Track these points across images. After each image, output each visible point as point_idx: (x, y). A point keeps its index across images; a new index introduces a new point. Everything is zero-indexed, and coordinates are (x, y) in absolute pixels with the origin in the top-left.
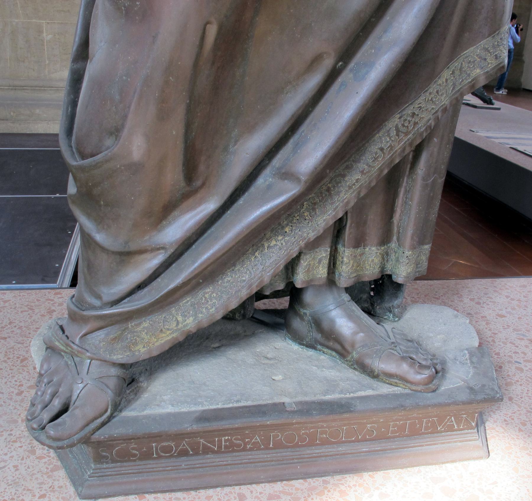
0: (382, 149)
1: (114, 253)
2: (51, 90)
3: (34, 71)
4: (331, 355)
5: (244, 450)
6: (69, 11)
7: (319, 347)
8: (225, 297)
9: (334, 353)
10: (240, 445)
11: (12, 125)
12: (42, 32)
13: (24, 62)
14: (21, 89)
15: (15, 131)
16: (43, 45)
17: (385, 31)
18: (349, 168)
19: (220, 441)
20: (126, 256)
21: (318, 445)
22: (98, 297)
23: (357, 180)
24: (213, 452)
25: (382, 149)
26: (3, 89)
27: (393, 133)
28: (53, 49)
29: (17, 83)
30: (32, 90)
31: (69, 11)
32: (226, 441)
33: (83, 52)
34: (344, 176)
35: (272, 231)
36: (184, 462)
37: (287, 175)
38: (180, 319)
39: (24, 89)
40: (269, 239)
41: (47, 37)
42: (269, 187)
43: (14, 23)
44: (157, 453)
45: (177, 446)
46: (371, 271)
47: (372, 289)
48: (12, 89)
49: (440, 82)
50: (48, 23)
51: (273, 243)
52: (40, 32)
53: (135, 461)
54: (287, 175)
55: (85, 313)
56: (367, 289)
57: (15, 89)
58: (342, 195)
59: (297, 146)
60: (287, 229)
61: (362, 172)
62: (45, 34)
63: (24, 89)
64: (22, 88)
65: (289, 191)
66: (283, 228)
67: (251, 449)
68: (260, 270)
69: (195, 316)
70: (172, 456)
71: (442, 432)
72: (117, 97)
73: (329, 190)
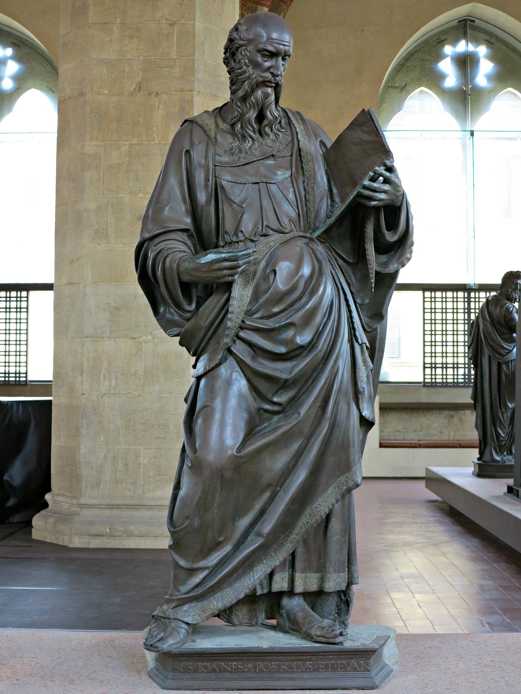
0: (304, 524)
1: (187, 569)
2: (144, 508)
3: (130, 491)
4: (297, 635)
5: (244, 671)
6: (164, 438)
7: (291, 632)
8: (236, 593)
9: (297, 634)
10: (241, 669)
11: (107, 540)
12: (140, 456)
13: (121, 483)
14: (117, 508)
15: (109, 546)
16: (140, 468)
17: (295, 474)
18: (290, 533)
19: (232, 665)
20: (192, 571)
21: (281, 672)
22: (179, 591)
23: (294, 538)
24: (229, 671)
25: (304, 524)
26: (101, 508)
27: (308, 516)
28: (149, 471)
29: (114, 502)
30: (127, 508)
31: (164, 438)
32: (235, 665)
33: (177, 487)
34: (288, 536)
35: (257, 562)
36: (213, 675)
37: (259, 534)
38: (215, 603)
39: (120, 508)
40: (256, 567)
41: (143, 460)
42: (252, 540)
43: (116, 450)
44: (201, 670)
45: (211, 666)
46: (314, 587)
47: (336, 613)
48: (109, 508)
49: (328, 492)
50: (146, 449)
51: (258, 568)
52: (138, 456)
53: (190, 673)
54: (259, 534)
55: (173, 598)
56: (334, 613)
57: (112, 508)
58: (288, 544)
59: (263, 522)
60: (264, 562)
61: (296, 535)
62: (142, 459)
63: (120, 508)
64: (118, 507)
65: (260, 541)
66: (262, 561)
67: (247, 672)
68: (252, 580)
69: (222, 602)
70: (208, 672)
71: (351, 671)
72: (190, 503)
73: (282, 543)
